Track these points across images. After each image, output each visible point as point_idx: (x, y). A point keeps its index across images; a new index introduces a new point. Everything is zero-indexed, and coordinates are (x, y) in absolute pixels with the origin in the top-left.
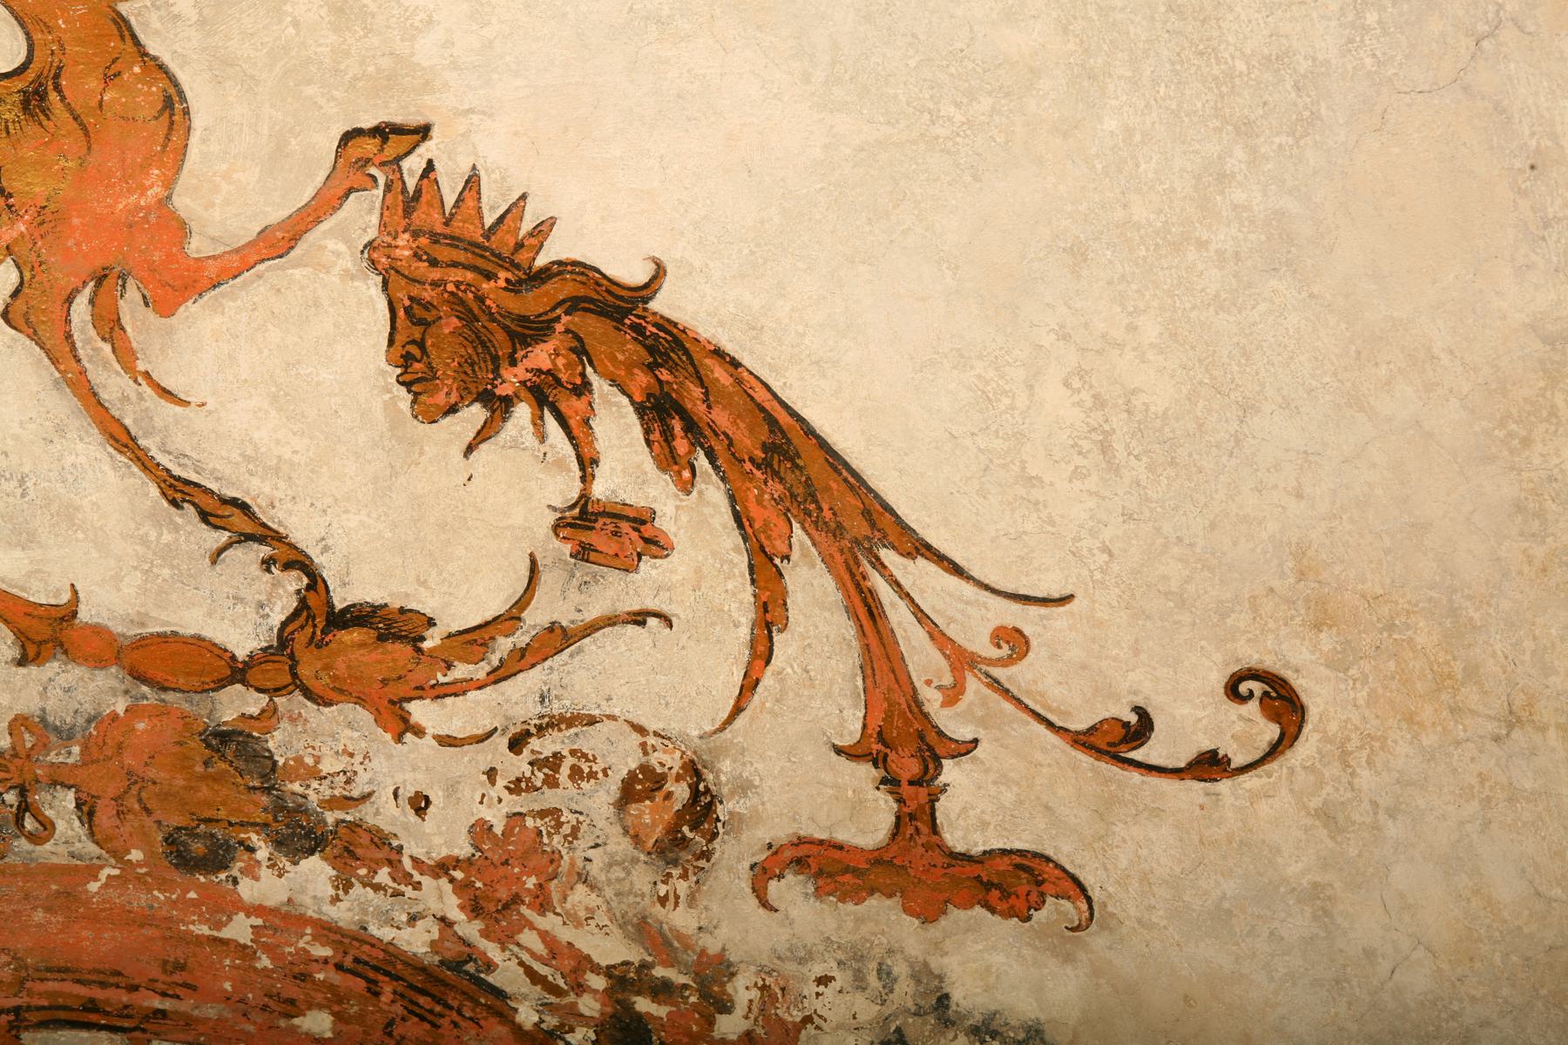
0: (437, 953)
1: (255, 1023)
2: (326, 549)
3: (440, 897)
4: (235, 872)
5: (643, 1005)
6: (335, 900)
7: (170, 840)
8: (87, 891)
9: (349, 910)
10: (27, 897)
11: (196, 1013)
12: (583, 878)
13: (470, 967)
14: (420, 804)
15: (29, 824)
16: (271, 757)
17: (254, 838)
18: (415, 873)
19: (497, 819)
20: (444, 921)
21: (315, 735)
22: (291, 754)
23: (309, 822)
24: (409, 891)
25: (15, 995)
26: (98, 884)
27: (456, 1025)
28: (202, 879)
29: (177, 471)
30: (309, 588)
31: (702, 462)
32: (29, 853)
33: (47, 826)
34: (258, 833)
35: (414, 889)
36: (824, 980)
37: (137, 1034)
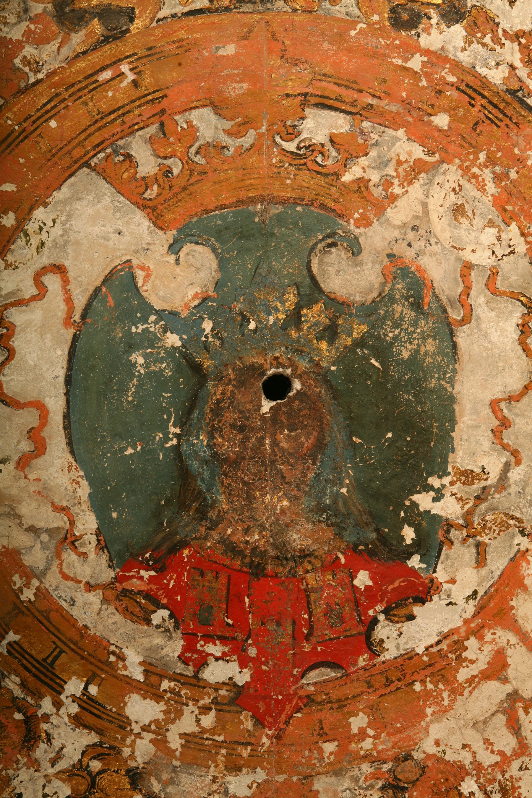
0: (506, 84)
1: (413, 117)
4: (420, 31)
6: (464, 49)
7: (393, 10)
8: (350, 35)
9: (469, 56)
10: (322, 34)
11: (387, 107)
13: (520, 94)
17: (432, 13)
18: (503, 38)
20: (512, 67)
23: (459, 4)
24: (498, 48)
25: (307, 87)
26: (356, 32)
27: (507, 126)
28: (403, 33)
32: (329, 10)
34: (434, 9)
35: (501, 48)
37: (358, 116)
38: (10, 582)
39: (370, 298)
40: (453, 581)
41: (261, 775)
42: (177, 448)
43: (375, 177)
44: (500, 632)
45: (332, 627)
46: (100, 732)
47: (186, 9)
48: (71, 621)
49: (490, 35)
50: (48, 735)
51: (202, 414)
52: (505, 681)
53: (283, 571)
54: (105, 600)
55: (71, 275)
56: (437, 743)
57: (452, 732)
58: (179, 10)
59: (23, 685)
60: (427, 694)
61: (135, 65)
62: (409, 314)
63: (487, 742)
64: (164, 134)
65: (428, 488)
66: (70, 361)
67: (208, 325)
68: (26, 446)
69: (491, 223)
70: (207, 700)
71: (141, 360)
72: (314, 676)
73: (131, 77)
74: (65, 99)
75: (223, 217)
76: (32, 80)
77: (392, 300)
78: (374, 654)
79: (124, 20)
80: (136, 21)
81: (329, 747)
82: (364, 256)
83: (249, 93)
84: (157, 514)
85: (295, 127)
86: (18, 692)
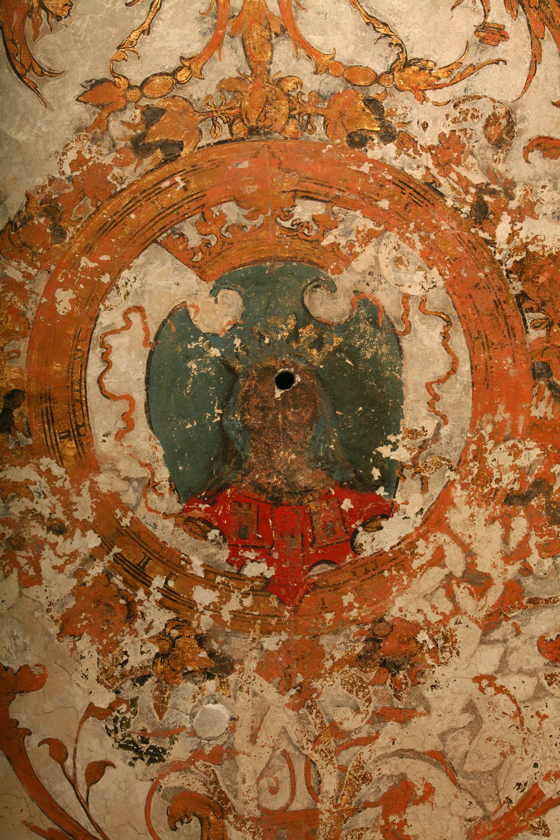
2: (408, 40)
3: (427, 160)
4: (367, 148)
5: (486, 198)
6: (396, 158)
7: (349, 136)
10: (304, 152)
12: (472, 153)
13: (434, 185)
14: (425, 126)
15: (309, 127)
16: (383, 108)
17: (374, 136)
19: (447, 132)
20: (428, 169)
21: (397, 101)
22: (389, 108)
24: (417, 156)
27: (427, 205)
29: (369, 13)
30: (402, 52)
31: (520, 9)
33: (314, 128)
36: (544, 187)
38: (114, 514)
39: (343, 320)
40: (406, 503)
41: (284, 636)
42: (220, 423)
43: (343, 242)
44: (439, 535)
45: (328, 537)
46: (176, 611)
47: (216, 141)
48: (155, 539)
49: (412, 149)
50: (143, 614)
51: (236, 400)
52: (444, 566)
53: (294, 501)
54: (176, 525)
55: (147, 312)
56: (401, 610)
57: (410, 602)
58: (212, 141)
59: (125, 581)
60: (392, 578)
61: (184, 176)
62: (370, 329)
63: (434, 607)
64: (205, 220)
65: (388, 442)
66: (148, 368)
67: (237, 342)
68: (121, 425)
69: (420, 268)
70: (246, 589)
71: (194, 366)
72: (317, 570)
73: (182, 184)
74: (140, 200)
75: (245, 271)
76: (119, 189)
77: (358, 320)
78: (357, 554)
79: (176, 149)
80: (184, 149)
81: (329, 616)
82: (339, 293)
83: (258, 191)
84: (209, 467)
85: (289, 211)
86: (121, 586)
